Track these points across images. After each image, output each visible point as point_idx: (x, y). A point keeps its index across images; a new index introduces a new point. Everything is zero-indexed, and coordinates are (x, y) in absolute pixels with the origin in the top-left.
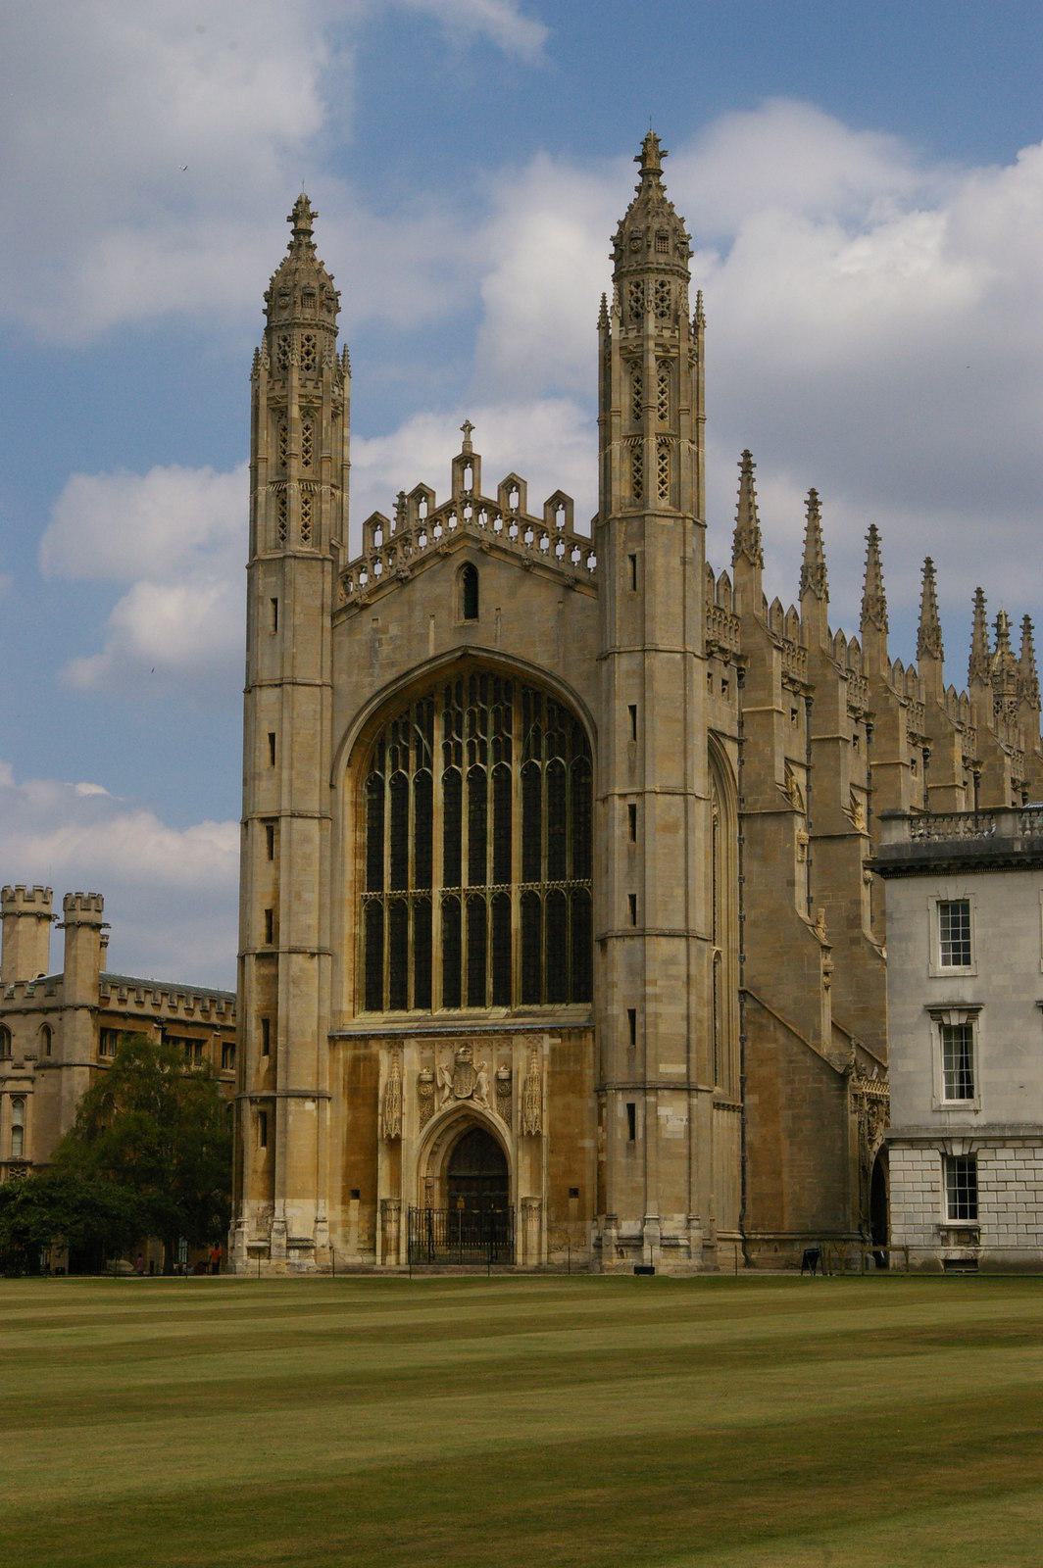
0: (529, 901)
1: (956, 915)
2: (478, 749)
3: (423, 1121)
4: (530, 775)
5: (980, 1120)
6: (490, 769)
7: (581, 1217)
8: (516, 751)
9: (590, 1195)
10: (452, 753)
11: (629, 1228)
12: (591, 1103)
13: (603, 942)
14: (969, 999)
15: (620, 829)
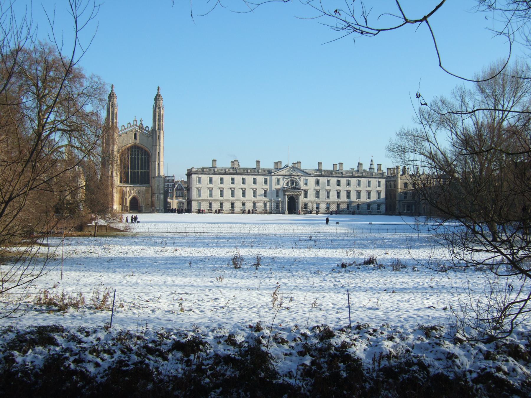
0: (141, 172)
1: (199, 179)
2: (135, 154)
3: (129, 196)
4: (142, 158)
5: (202, 199)
6: (136, 157)
7: (149, 207)
8: (140, 155)
9: (150, 205)
10: (131, 154)
11: (158, 208)
12: (150, 195)
13: (154, 178)
14: (200, 187)
15: (157, 166)
